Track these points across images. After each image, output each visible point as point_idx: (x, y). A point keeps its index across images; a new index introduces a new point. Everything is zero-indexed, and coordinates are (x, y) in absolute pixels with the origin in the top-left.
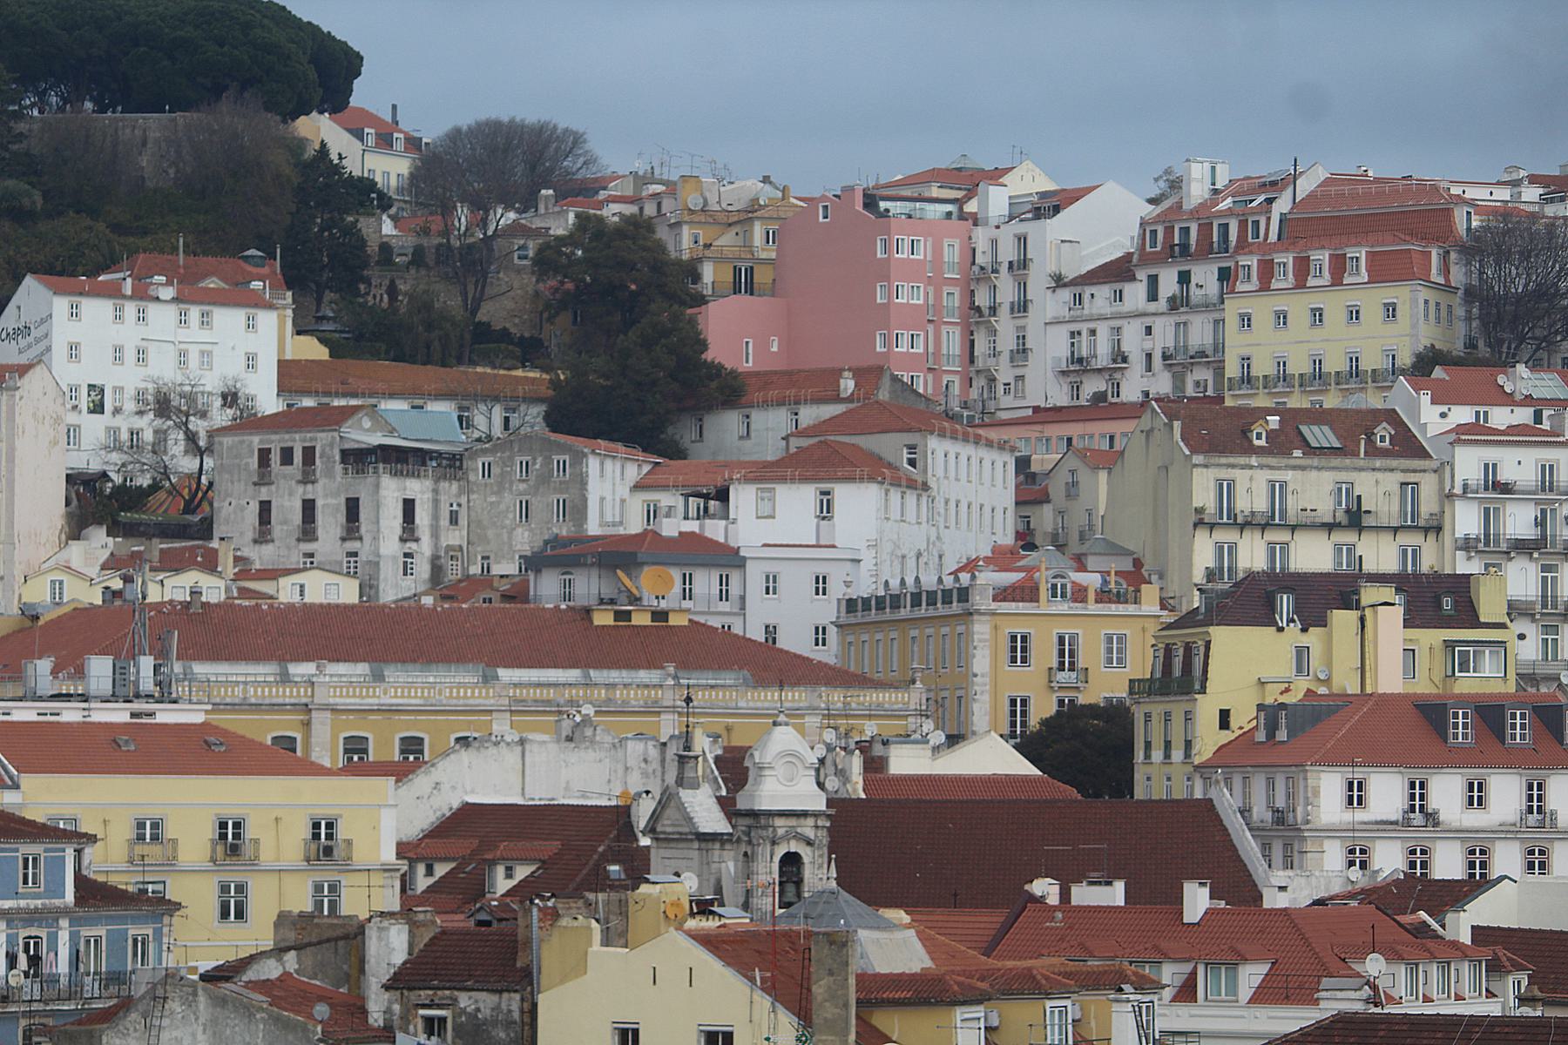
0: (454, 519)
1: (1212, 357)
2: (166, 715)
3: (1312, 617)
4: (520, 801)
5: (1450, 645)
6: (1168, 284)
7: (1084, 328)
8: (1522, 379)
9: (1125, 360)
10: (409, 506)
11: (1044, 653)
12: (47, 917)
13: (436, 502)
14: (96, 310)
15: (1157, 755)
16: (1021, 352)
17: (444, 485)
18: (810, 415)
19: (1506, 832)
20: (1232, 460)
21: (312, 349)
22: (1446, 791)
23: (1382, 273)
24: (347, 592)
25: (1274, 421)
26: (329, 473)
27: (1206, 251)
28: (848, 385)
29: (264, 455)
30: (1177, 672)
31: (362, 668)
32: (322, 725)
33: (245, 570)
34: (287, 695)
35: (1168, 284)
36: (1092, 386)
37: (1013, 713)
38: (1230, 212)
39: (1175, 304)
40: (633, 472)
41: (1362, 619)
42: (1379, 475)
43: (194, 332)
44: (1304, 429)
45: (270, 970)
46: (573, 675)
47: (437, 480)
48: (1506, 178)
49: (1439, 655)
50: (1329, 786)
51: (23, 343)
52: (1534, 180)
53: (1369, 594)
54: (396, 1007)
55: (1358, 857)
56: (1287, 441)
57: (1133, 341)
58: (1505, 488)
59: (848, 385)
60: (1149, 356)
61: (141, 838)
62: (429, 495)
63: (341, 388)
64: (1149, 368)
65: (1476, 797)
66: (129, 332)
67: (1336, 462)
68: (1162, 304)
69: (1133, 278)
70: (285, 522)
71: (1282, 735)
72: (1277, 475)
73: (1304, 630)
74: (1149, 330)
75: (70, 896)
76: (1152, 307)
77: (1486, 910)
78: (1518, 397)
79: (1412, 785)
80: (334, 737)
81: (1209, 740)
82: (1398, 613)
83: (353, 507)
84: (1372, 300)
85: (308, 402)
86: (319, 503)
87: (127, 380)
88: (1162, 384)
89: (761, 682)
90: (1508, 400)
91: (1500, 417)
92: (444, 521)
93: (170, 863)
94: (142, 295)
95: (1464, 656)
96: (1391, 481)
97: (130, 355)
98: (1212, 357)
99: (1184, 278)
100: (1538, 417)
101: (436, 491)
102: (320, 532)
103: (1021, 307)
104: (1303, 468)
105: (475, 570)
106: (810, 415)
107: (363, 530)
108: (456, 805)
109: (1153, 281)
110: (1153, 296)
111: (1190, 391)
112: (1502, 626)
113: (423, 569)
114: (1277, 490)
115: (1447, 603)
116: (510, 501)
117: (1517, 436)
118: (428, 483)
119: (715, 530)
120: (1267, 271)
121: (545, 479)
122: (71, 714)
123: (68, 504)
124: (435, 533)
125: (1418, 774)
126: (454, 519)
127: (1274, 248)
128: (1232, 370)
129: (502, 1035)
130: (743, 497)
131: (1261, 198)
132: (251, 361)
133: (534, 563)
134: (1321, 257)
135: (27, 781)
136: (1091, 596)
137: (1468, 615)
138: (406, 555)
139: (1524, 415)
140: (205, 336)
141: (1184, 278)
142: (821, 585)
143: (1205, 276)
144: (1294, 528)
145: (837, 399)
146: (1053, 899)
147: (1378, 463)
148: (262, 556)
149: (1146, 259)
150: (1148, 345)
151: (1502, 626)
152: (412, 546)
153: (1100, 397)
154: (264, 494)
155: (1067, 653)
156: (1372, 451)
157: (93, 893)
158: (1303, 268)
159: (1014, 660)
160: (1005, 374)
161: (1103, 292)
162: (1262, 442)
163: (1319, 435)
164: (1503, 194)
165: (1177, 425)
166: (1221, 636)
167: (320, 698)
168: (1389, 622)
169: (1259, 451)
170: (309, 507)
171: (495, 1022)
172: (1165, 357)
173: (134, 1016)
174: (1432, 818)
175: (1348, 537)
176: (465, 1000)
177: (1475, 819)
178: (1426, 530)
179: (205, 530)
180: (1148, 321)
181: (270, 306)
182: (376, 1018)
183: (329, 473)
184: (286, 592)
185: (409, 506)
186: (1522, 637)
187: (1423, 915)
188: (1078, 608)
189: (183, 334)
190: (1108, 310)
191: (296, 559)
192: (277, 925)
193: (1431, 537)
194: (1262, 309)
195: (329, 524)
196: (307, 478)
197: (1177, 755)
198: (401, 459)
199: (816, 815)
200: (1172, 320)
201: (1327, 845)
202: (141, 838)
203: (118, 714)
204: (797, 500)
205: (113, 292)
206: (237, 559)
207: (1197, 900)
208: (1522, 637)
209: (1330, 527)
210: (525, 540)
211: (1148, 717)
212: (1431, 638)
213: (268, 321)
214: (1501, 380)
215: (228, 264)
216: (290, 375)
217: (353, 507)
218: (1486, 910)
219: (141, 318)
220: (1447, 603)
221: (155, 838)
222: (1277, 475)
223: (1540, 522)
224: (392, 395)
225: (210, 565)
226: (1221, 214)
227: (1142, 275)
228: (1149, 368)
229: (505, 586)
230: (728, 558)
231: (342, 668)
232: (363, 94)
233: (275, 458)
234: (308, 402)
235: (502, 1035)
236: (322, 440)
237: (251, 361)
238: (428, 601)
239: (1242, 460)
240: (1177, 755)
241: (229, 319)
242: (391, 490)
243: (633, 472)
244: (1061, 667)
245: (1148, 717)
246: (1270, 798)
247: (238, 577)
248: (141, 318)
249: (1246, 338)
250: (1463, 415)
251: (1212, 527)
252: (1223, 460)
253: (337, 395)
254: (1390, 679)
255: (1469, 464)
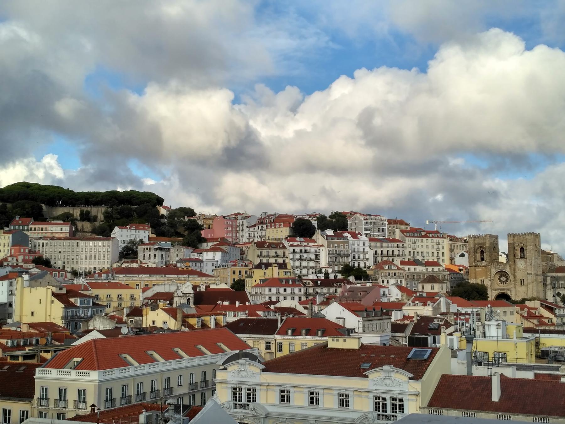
0: (168, 257)
1: (265, 236)
2: (113, 281)
3: (266, 268)
4: (164, 292)
5: (284, 271)
6: (260, 227)
7: (250, 233)
8: (298, 239)
9: (255, 237)
10: (162, 255)
11: (237, 273)
12: (88, 308)
13: (166, 255)
14: (124, 231)
15: (248, 286)
16: (243, 236)
17: (167, 252)
18: (215, 243)
19: (289, 295)
20: (262, 249)
21: (154, 236)
22: (281, 290)
23: (285, 226)
24: (154, 266)
25: (268, 244)
26: (152, 251)
27: (265, 224)
28: (219, 240)
29: (144, 249)
30: (250, 275)
31: (149, 275)
32: (142, 282)
33: (141, 263)
34: (138, 279)
35: (260, 227)
36: (251, 240)
37: (233, 280)
38: (268, 219)
39: (261, 230)
40: (191, 251)
41: (273, 268)
42: (280, 251)
43: (137, 233)
44: (271, 245)
45: (112, 314)
46: (176, 276)
47: (166, 252)
48: (305, 215)
49: (283, 273)
50: (267, 289)
51: (115, 235)
52: (308, 215)
53: (274, 265)
54: (127, 319)
55: (270, 298)
56: (268, 247)
57: (256, 235)
58: (296, 252)
59: (219, 240)
60: (258, 236)
61: (108, 297)
62: (165, 253)
63: (156, 240)
64: (258, 238)
65: (285, 290)
66: (129, 234)
67: (275, 249)
68: (259, 230)
69: (256, 227)
70: (147, 257)
71: (262, 283)
72: (268, 251)
73: (266, 270)
74: (258, 233)
75: (91, 305)
76: (258, 230)
77: (278, 305)
78: (298, 241)
79: (277, 289)
80: (144, 284)
81: (254, 284)
82: (277, 267)
83: (155, 255)
84: (284, 229)
85: (152, 242)
86: (151, 255)
87: (128, 239)
88: (259, 240)
89: (199, 276)
90: (297, 241)
91: (296, 243)
92: (167, 257)
93: (112, 300)
94: (130, 228)
95: (285, 273)
96: (282, 251)
97: (129, 236)
98: (265, 236)
99: (262, 227)
100: (300, 244)
101: (166, 253)
102: (151, 258)
103: (243, 230)
104: (271, 250)
105: (171, 263)
106: (215, 243)
107: (156, 258)
108: (156, 293)
109: (258, 227)
110: (258, 229)
111: (263, 241)
112: (290, 269)
113: (164, 263)
114: (268, 253)
115: (284, 266)
116: (175, 254)
117: (298, 246)
118: (165, 252)
119: (201, 258)
120: (271, 226)
121: (180, 252)
122: (100, 281)
123: (119, 254)
124: (166, 258)
125: (278, 288)
126: (168, 257)
127: (272, 223)
128: (267, 238)
129: (140, 322)
130: (204, 253)
131: (271, 217)
132: (145, 237)
133: (177, 262)
134: (277, 224)
135: (93, 290)
136: (243, 266)
137: (286, 268)
138: (162, 261)
139: (299, 243)
140: (139, 234)
141: (262, 227)
142: (213, 264)
143: (264, 226)
144: (270, 257)
145: (218, 242)
146: (221, 304)
147: (280, 249)
148: (144, 261)
149: (258, 224)
150: (258, 235)
151: (290, 269)
152: (163, 260)
153: (252, 241)
154: (144, 253)
155: (240, 272)
156: (280, 248)
157: (94, 304)
158: (275, 226)
159: (233, 274)
160: (241, 239)
161: (252, 228)
162: (266, 247)
163: (273, 246)
164: (304, 217)
165: (256, 244)
166: (255, 270)
167: (143, 279)
168: (276, 268)
169: (266, 248)
170: (150, 255)
171: (139, 321)
172: (260, 236)
173: (92, 320)
174: (280, 293)
175: (277, 258)
176: (135, 318)
177: (285, 293)
178: (286, 257)
179: (137, 258)
180: (258, 232)
181: (147, 230)
182: (124, 320)
183: (152, 251)
184: (146, 266)
185: (162, 255)
186: (298, 271)
187: (269, 305)
188: (241, 267)
189: (136, 234)
190: (253, 231)
191: (148, 262)
192: (113, 308)
193: (287, 258)
194: (271, 230)
195: (152, 257)
196: (150, 251)
197: (250, 285)
198: (161, 249)
199: (192, 293)
200: (260, 232)
201: (266, 297)
202: (108, 297)
203: (106, 281)
204: (211, 254)
205: (127, 228)
206: (140, 262)
207: (237, 304)
208: (298, 271)
209: (275, 257)
210: (177, 259)
211: (247, 281)
212: (281, 271)
213: (147, 232)
214: (296, 239)
215: (143, 225)
216: (150, 239)
217: (155, 255)
218: (278, 305)
219: (130, 232)
220: (284, 266)
221: (109, 297)
222: (268, 251)
223: (300, 257)
224: (163, 241)
225: (137, 263)
226: (266, 219)
227: (257, 226)
228: (258, 238)
229: (175, 265)
230: (201, 261)
231: (146, 275)
232: (164, 204)
233: (146, 249)
234: (152, 242)
235: (140, 322)
236: (152, 247)
237: (145, 237)
238: (164, 267)
239: (264, 249)
240: (250, 285)
241: (142, 232)
242: (159, 253)
243: (191, 251)
244: (239, 275)
245: (247, 281)
246: (260, 290)
247: (140, 264)
248: (130, 232)
249: (269, 234)
250: (291, 243)
251: (260, 257)
252: (261, 249)
253: (156, 241)
254: (276, 276)
255: (291, 249)
